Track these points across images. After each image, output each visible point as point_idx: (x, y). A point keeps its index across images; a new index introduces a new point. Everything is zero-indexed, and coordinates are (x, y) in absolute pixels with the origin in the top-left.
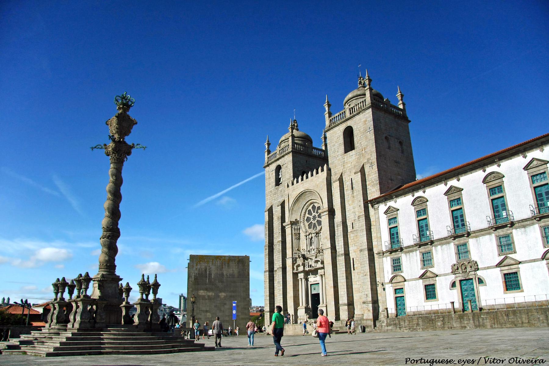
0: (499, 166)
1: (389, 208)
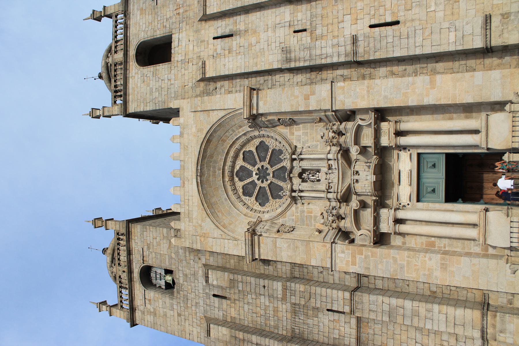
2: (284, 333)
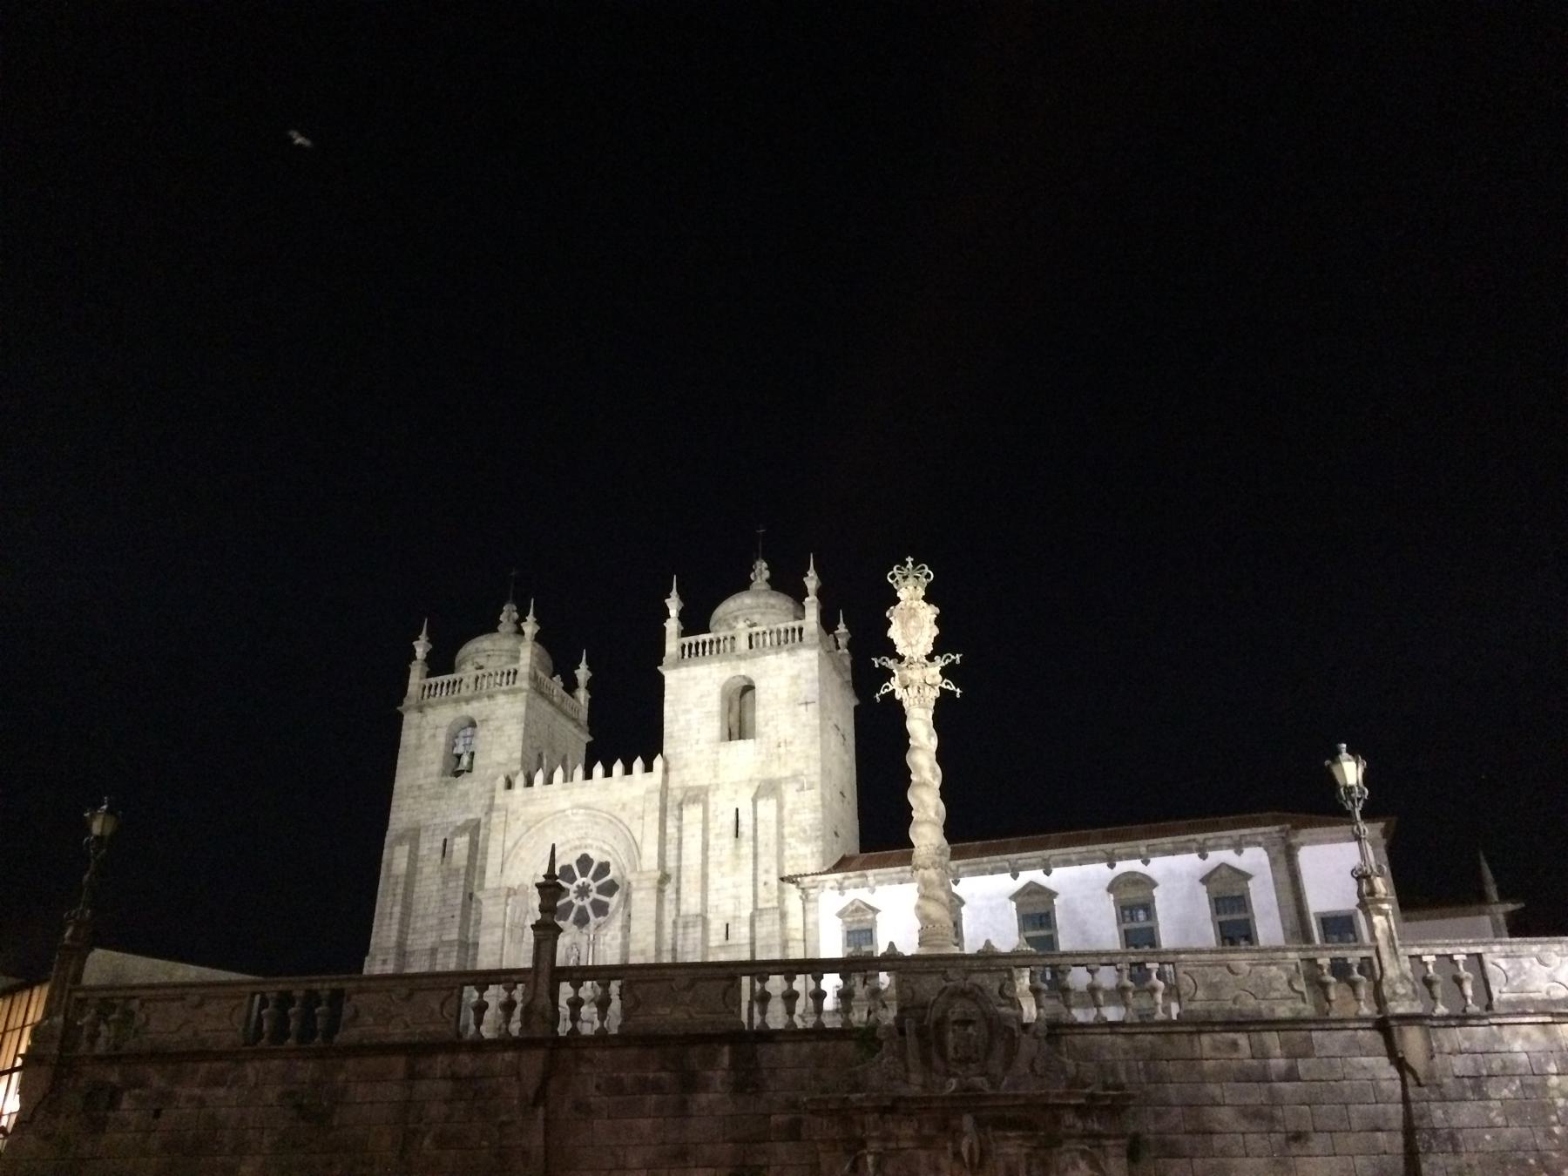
0: (1146, 862)
1: (852, 903)
2: (409, 942)
